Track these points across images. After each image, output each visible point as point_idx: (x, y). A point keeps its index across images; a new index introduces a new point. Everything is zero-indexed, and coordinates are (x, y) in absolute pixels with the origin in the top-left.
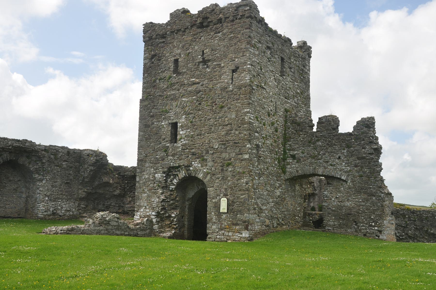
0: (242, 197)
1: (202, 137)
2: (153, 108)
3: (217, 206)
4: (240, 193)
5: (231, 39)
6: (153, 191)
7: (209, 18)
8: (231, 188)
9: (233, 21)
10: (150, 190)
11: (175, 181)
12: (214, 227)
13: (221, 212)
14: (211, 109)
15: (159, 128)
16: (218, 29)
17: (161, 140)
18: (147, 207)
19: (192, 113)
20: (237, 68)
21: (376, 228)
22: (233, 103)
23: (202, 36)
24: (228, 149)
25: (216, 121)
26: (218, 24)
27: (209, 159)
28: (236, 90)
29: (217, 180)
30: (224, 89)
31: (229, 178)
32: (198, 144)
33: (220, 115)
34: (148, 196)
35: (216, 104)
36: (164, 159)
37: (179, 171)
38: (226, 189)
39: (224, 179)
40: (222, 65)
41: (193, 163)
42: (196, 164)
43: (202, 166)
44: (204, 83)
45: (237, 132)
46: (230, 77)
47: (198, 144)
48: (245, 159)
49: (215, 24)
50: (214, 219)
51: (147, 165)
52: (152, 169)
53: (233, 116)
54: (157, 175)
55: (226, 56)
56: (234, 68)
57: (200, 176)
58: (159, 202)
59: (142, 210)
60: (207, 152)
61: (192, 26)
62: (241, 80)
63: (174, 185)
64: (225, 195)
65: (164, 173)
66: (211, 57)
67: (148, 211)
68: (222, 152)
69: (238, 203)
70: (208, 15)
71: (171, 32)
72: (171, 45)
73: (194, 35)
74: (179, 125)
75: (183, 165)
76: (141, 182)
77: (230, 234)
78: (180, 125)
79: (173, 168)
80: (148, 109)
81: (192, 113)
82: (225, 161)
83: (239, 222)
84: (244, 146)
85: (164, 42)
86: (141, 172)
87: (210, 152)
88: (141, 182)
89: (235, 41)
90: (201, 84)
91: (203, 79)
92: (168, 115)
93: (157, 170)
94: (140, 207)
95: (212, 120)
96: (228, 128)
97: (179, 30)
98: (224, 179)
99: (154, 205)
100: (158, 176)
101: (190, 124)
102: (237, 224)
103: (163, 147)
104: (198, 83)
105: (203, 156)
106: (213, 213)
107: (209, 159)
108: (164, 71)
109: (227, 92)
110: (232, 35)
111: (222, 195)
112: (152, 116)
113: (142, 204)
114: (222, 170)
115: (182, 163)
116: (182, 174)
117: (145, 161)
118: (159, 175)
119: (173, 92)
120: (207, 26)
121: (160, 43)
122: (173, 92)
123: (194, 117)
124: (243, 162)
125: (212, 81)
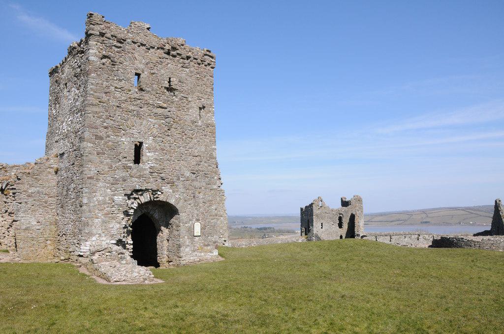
0: (212, 221)
1: (172, 163)
2: (108, 118)
3: (191, 230)
4: (212, 217)
5: (198, 79)
6: (110, 215)
7: (178, 49)
8: (203, 213)
9: (199, 64)
10: (106, 214)
11: (135, 205)
12: (187, 250)
13: (195, 235)
14: (181, 138)
15: (116, 145)
16: (185, 64)
17: (121, 158)
18: (103, 235)
19: (159, 137)
20: (204, 107)
21: (223, 239)
22: (201, 137)
23: (169, 63)
24: (198, 178)
25: (186, 150)
26: (185, 59)
27: (181, 186)
28: (205, 126)
29: (189, 206)
30: (193, 122)
31: (201, 205)
32: (168, 169)
33: (190, 145)
34: (104, 222)
35: (186, 135)
36: (125, 180)
37: (142, 195)
38: (197, 215)
39: (196, 205)
40: (190, 99)
41: (163, 188)
42: (167, 189)
43: (174, 192)
44: (172, 109)
45: (206, 165)
46: (198, 113)
47: (168, 169)
48: (214, 189)
49: (182, 58)
50: (187, 243)
51: (100, 184)
52: (109, 190)
53: (203, 150)
54: (116, 198)
55: (193, 93)
56: (201, 107)
57: (172, 201)
58: (120, 228)
59: (94, 238)
60: (178, 179)
61: (158, 48)
62: (208, 120)
63: (132, 208)
64: (198, 220)
65: (125, 195)
66: (178, 88)
67: (104, 239)
68: (193, 180)
69: (209, 226)
70: (178, 47)
71: (133, 42)
72: (130, 55)
73: (160, 58)
74: (145, 146)
75: (151, 189)
76: (92, 205)
77: (202, 254)
78: (147, 145)
79: (137, 191)
80: (100, 117)
81: (159, 137)
82: (196, 188)
83: (210, 243)
84: (213, 178)
85: (120, 47)
86: (90, 193)
87: (181, 179)
88: (92, 205)
89: (201, 83)
90: (168, 110)
91: (171, 106)
92: (131, 131)
93: (116, 192)
94: (90, 234)
95: (181, 148)
96: (198, 159)
97: (143, 45)
98: (196, 205)
99: (114, 232)
100: (120, 198)
101: (158, 148)
102: (208, 245)
103: (123, 166)
104: (166, 108)
105: (173, 183)
106: (186, 237)
107: (181, 186)
108: (120, 80)
109: (196, 126)
110: (198, 76)
111: (194, 220)
112: (106, 128)
113: (94, 231)
114: (194, 197)
115: (149, 186)
116: (145, 198)
117: (98, 180)
118: (120, 197)
119: (133, 108)
120: (174, 56)
121: (115, 46)
122: (133, 108)
123: (163, 141)
124: (212, 192)
125: (180, 110)
